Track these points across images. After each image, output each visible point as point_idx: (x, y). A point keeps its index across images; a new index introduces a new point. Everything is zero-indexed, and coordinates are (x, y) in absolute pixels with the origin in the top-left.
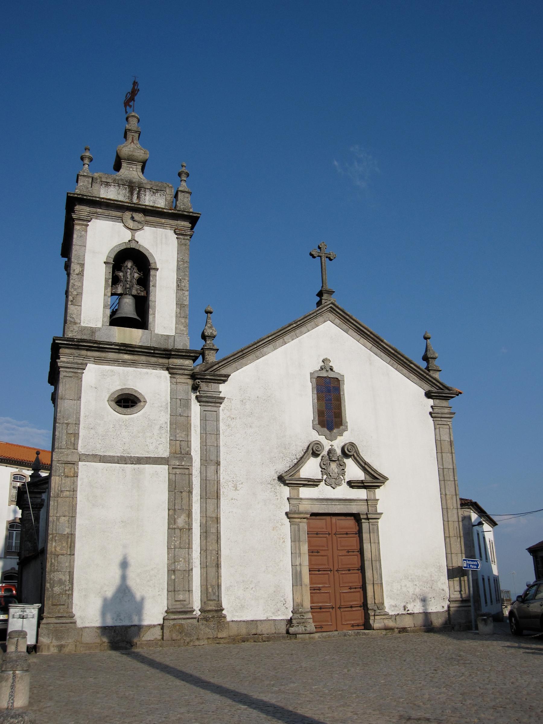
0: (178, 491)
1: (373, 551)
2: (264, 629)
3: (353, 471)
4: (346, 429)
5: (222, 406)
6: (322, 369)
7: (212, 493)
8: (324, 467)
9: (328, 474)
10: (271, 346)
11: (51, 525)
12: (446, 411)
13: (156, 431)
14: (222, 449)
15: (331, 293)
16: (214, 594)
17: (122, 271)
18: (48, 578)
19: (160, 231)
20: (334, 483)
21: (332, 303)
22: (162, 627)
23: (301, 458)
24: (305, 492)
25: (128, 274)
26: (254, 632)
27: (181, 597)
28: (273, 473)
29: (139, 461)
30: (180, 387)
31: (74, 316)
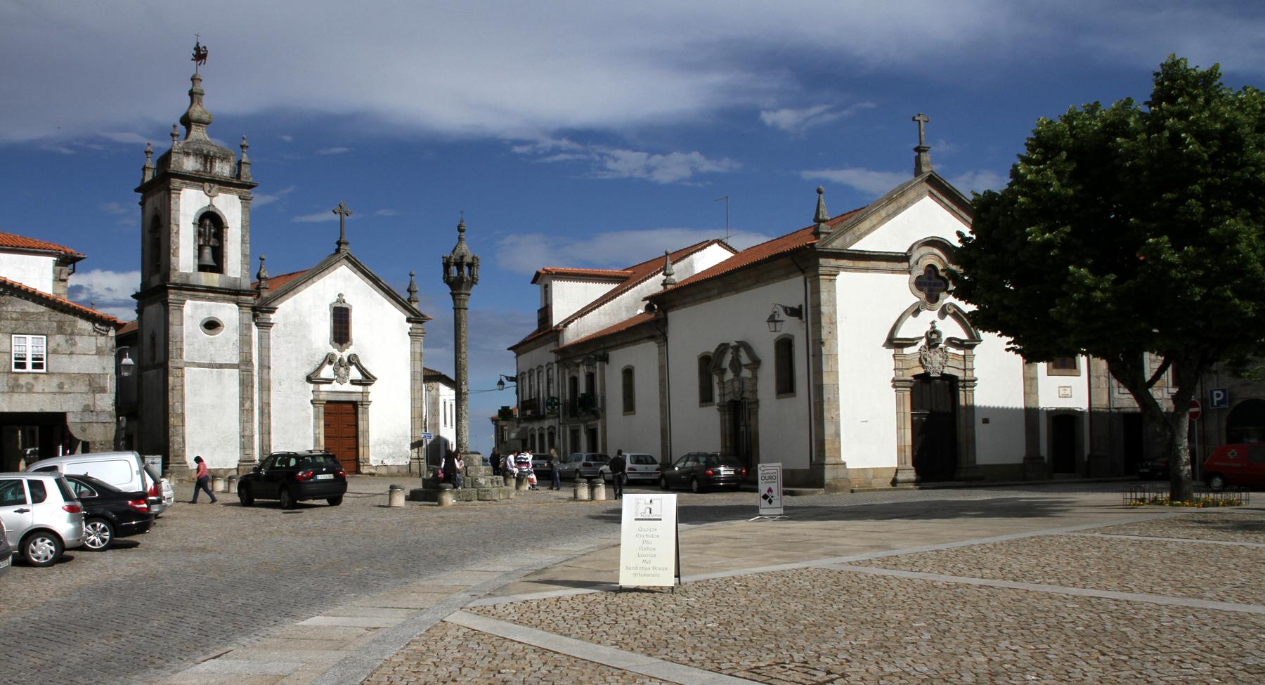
0: (245, 384)
3: (355, 374)
7: (265, 387)
15: (346, 244)
19: (229, 196)
20: (341, 380)
22: (238, 470)
24: (323, 387)
29: (221, 366)
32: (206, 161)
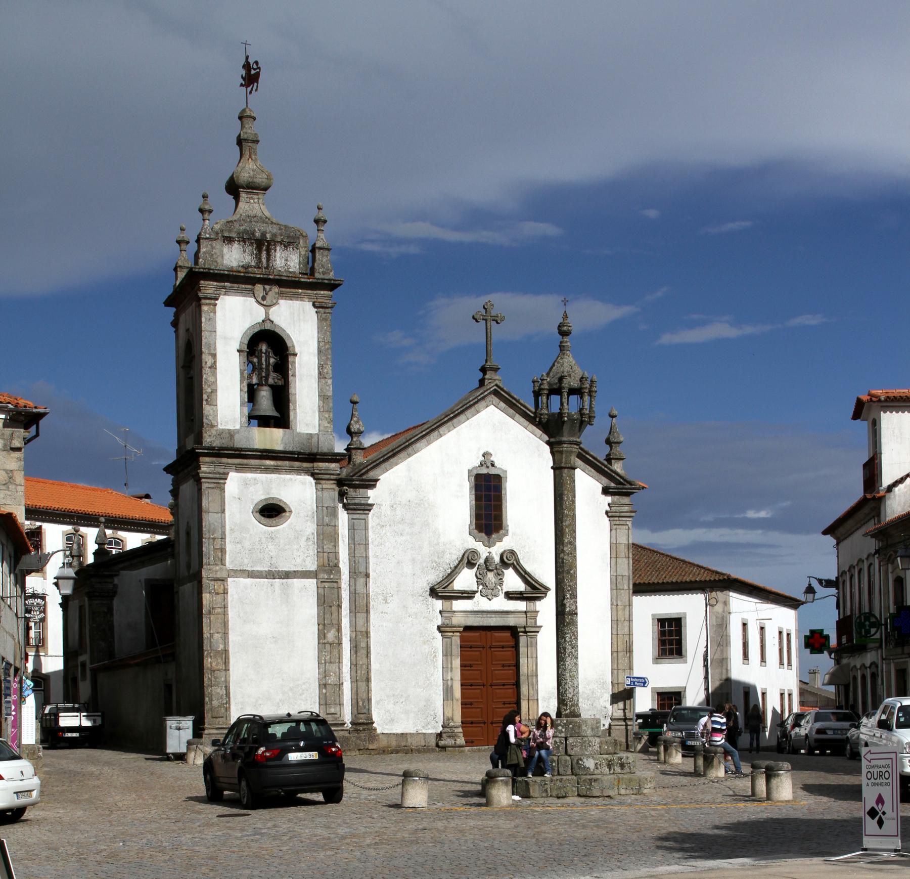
0: (327, 604)
1: (530, 666)
2: (414, 743)
3: (512, 581)
4: (506, 534)
5: (371, 513)
6: (482, 465)
7: (361, 607)
8: (479, 576)
9: (484, 585)
10: (424, 441)
11: (205, 642)
12: (626, 508)
13: (303, 542)
14: (372, 560)
15: (496, 370)
16: (365, 707)
17: (256, 357)
18: (206, 692)
19: (296, 304)
21: (496, 385)
23: (456, 567)
24: (459, 605)
25: (264, 359)
26: (403, 744)
27: (332, 710)
28: (425, 584)
29: (287, 575)
30: (326, 494)
31: (211, 418)
32: (259, 249)
